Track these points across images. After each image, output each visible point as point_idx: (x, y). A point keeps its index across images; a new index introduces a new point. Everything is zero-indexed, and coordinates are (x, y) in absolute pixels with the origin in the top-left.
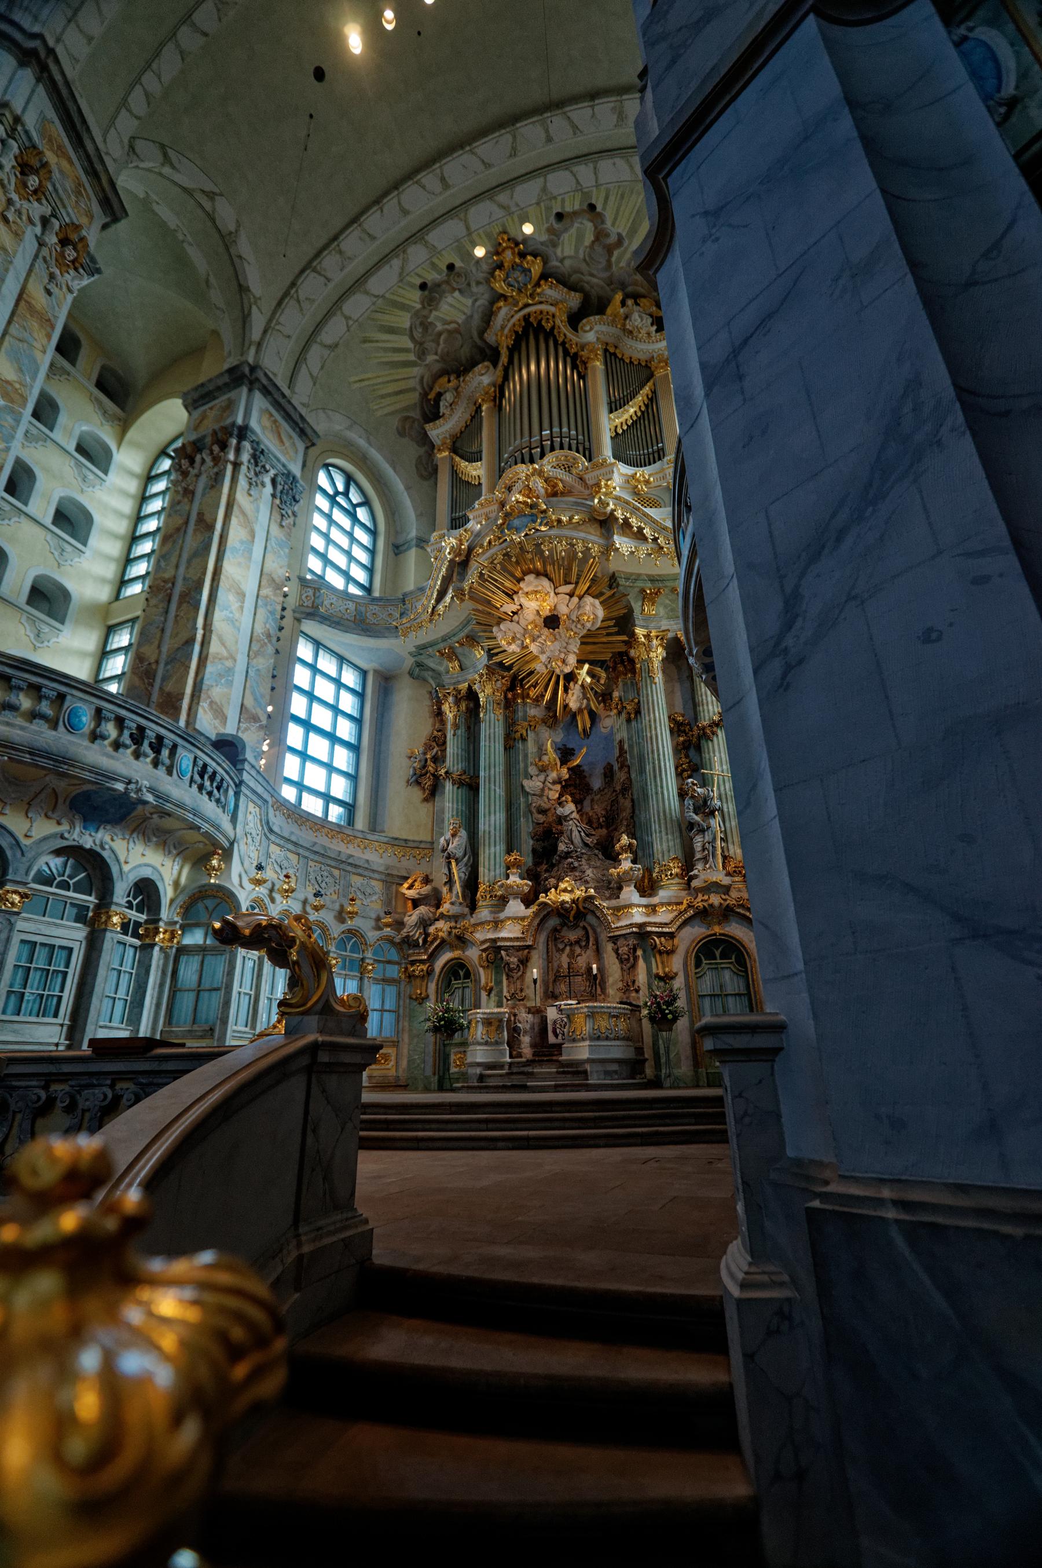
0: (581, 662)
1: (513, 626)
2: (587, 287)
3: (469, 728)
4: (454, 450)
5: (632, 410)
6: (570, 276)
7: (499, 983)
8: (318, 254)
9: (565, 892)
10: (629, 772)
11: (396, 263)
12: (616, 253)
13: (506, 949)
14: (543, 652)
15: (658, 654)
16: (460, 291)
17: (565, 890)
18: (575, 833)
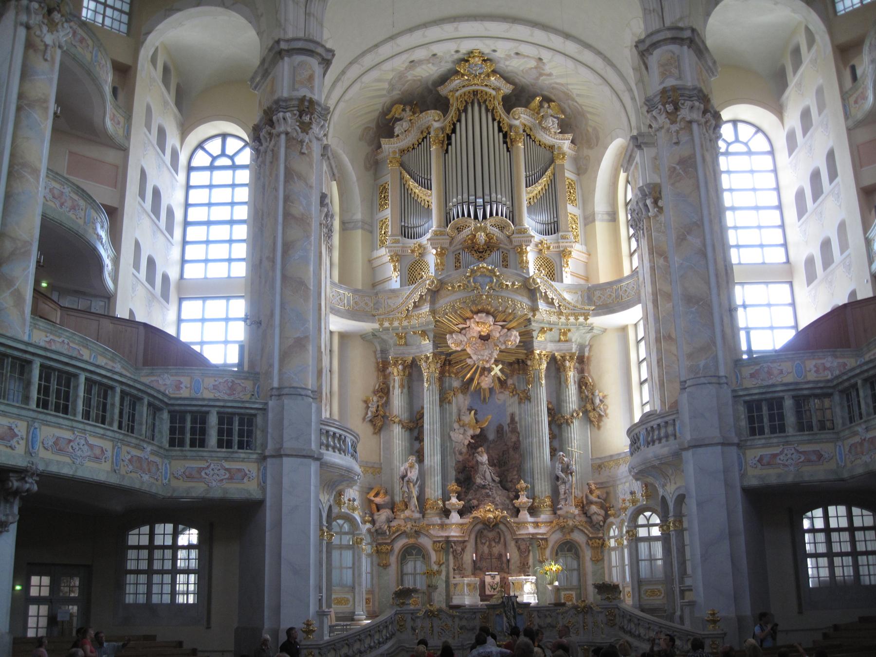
0: (497, 362)
1: (461, 337)
2: (517, 81)
3: (409, 388)
4: (402, 165)
5: (540, 188)
6: (508, 72)
7: (447, 560)
8: (363, 54)
9: (488, 511)
10: (519, 437)
11: (404, 57)
12: (544, 77)
13: (455, 542)
14: (475, 354)
15: (544, 366)
16: (433, 64)
17: (489, 511)
18: (488, 473)
